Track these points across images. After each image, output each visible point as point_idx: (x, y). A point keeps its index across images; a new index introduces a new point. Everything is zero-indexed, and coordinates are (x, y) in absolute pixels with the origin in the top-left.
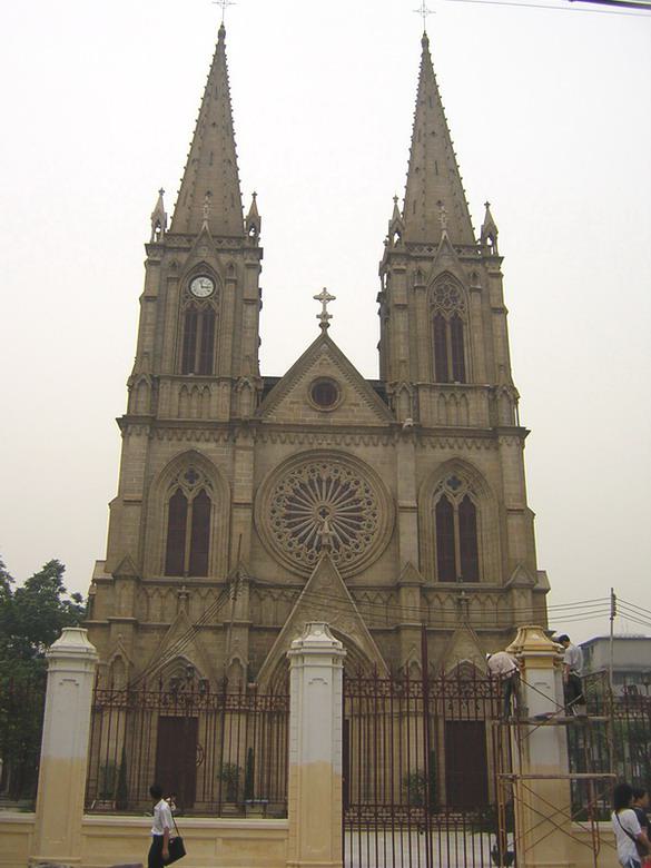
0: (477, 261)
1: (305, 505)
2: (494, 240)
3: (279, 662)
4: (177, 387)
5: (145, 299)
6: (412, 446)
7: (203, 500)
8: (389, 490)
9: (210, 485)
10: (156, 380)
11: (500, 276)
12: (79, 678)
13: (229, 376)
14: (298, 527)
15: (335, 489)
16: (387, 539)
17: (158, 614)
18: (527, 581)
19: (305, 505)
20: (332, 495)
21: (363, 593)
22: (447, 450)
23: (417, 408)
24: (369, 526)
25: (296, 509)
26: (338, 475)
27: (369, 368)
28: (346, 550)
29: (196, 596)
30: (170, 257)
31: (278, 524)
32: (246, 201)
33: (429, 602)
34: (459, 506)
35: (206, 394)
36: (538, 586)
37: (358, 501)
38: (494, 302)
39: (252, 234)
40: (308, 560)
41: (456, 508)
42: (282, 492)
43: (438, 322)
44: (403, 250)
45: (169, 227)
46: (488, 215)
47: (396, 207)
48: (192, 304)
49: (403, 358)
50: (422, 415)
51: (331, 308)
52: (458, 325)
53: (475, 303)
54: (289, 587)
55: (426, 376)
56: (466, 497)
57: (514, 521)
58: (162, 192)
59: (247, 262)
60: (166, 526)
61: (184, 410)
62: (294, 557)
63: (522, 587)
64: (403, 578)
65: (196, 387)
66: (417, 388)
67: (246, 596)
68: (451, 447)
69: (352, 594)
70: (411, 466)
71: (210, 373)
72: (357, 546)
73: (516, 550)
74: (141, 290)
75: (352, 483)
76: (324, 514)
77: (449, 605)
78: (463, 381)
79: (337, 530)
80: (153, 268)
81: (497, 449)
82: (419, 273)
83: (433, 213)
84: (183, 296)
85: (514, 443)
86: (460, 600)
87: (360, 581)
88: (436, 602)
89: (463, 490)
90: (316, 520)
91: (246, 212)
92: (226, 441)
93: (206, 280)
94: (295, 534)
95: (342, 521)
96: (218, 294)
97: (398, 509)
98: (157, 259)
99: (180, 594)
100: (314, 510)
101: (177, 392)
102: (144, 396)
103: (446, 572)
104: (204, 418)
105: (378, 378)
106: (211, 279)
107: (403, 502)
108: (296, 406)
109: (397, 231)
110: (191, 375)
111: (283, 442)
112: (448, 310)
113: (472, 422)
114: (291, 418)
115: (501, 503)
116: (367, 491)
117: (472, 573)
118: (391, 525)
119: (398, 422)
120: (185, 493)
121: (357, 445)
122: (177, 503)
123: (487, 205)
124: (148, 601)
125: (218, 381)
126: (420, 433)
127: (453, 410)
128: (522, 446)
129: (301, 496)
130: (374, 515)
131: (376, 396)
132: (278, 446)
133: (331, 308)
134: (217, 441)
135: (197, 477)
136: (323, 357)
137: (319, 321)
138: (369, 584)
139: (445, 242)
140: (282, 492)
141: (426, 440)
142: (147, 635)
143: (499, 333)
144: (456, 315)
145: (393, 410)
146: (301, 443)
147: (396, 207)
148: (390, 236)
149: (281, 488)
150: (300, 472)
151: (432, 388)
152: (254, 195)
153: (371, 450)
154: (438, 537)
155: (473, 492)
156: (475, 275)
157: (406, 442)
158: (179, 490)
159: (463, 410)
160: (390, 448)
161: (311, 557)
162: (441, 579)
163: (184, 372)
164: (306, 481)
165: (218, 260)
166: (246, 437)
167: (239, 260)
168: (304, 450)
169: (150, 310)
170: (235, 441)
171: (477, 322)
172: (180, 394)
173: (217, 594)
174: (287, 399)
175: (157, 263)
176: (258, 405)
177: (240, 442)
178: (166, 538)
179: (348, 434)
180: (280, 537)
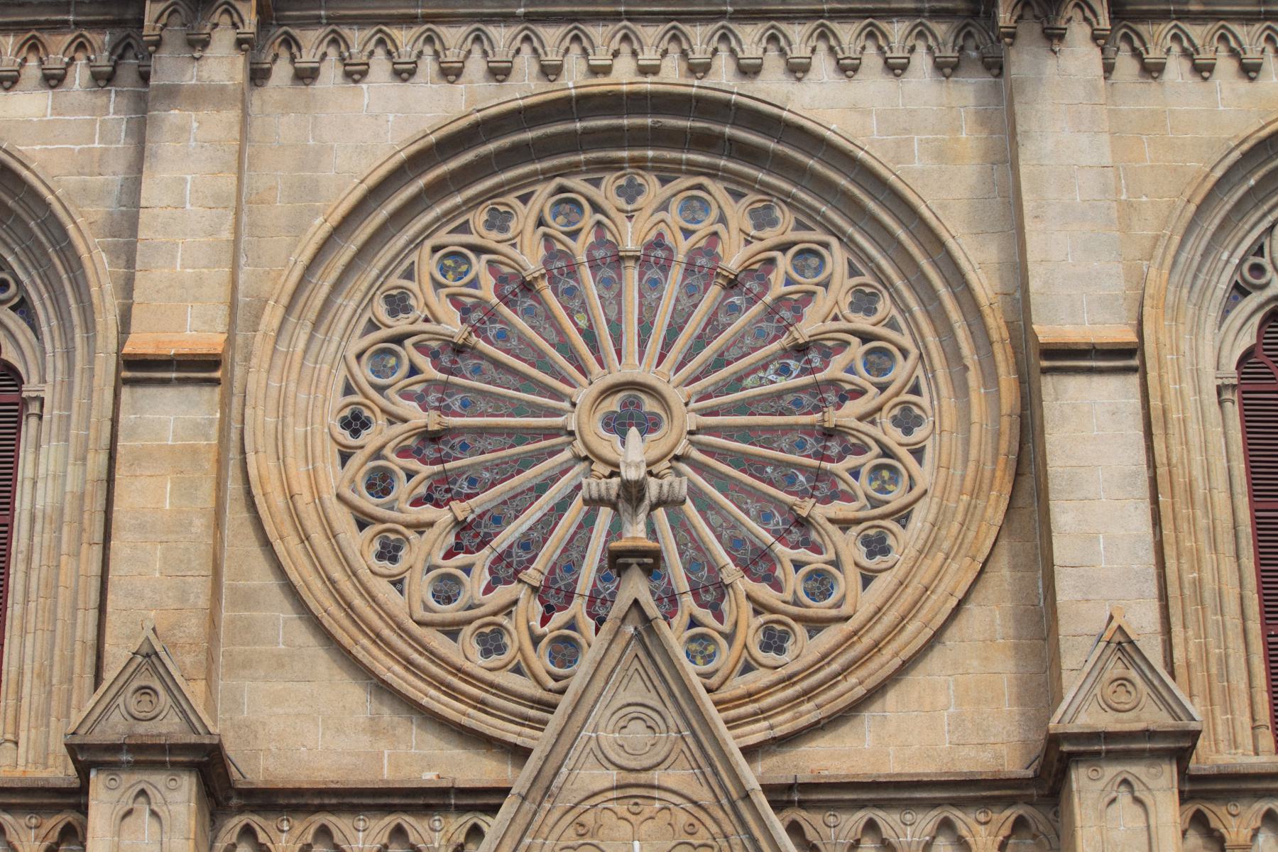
1: (526, 382)
8: (985, 286)
14: (485, 500)
15: (692, 291)
19: (526, 382)
21: (861, 817)
26: (703, 229)
28: (759, 608)
31: (380, 483)
40: (541, 662)
42: (401, 324)
62: (477, 663)
69: (795, 829)
72: (820, 584)
75: (784, 262)
90: (588, 459)
92: (102, 79)
107: (1047, 330)
111: (404, 74)
121: (798, 70)
130: (907, 421)
134: (53, 80)
138: (893, 766)
141: (1158, 37)
146: (499, 73)
150: (498, 221)
154: (1257, 522)
157: (1053, 37)
164: (531, 259)
166: (198, 44)
170: (145, 77)
180: (389, 552)
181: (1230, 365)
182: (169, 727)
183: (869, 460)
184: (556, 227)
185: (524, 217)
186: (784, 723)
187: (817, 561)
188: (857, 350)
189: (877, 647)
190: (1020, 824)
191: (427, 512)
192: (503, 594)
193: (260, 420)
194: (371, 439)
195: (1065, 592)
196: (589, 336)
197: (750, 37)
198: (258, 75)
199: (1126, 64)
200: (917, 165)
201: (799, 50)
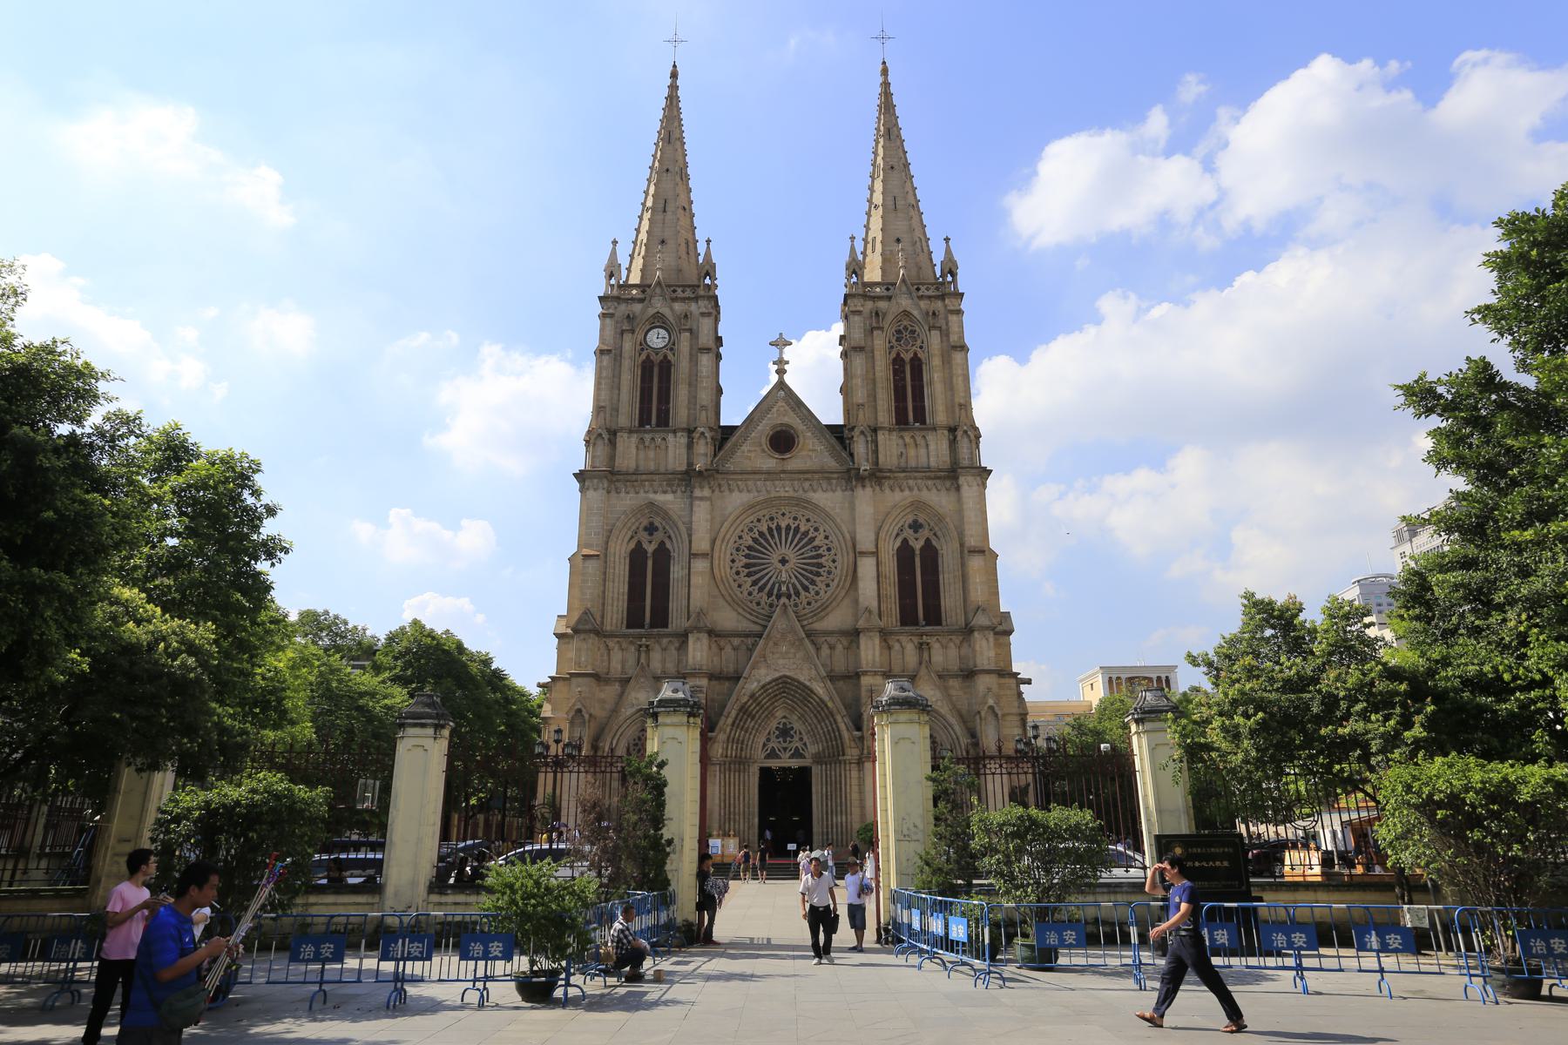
0: (937, 297)
1: (764, 554)
2: (953, 275)
3: (740, 710)
4: (634, 438)
5: (601, 353)
6: (871, 489)
7: (663, 555)
8: (848, 536)
9: (669, 537)
10: (613, 433)
11: (959, 312)
12: (428, 743)
13: (684, 426)
16: (848, 584)
17: (619, 667)
18: (987, 623)
19: (764, 554)
20: (792, 541)
22: (907, 493)
23: (876, 452)
24: (829, 573)
25: (755, 558)
26: (797, 523)
27: (830, 411)
29: (657, 647)
30: (623, 309)
31: (738, 573)
32: (701, 248)
33: (890, 648)
34: (921, 549)
35: (663, 447)
36: (1000, 628)
37: (817, 548)
38: (954, 338)
39: (708, 281)
40: (767, 608)
41: (918, 552)
43: (898, 362)
44: (860, 291)
45: (624, 278)
46: (948, 251)
47: (853, 249)
48: (648, 357)
49: (861, 401)
50: (880, 456)
51: (788, 353)
52: (917, 365)
53: (935, 339)
54: (747, 636)
55: (885, 416)
56: (928, 540)
57: (975, 563)
58: (615, 242)
59: (701, 310)
60: (627, 579)
61: (642, 463)
62: (755, 608)
63: (983, 628)
64: (861, 624)
65: (653, 439)
66: (875, 430)
67: (705, 647)
68: (911, 489)
69: (813, 643)
70: (870, 510)
71: (667, 425)
72: (817, 593)
73: (978, 594)
74: (595, 343)
75: (812, 530)
76: (783, 561)
77: (910, 648)
78: (923, 422)
79: (796, 577)
80: (608, 321)
81: (958, 489)
82: (877, 314)
83: (891, 251)
84: (638, 348)
85: (975, 483)
86: (921, 644)
87: (818, 626)
88: (897, 646)
89: (925, 533)
91: (701, 259)
93: (661, 330)
94: (754, 583)
95: (803, 569)
96: (674, 344)
97: (858, 554)
98: (611, 311)
99: (640, 646)
100: (775, 558)
101: (633, 446)
102: (602, 449)
103: (908, 617)
104: (662, 470)
105: (841, 422)
106: (667, 330)
108: (753, 455)
109: (854, 272)
110: (648, 427)
112: (907, 351)
113: (933, 464)
114: (748, 466)
115: (962, 545)
116: (826, 537)
117: (934, 616)
118: (850, 573)
119: (856, 466)
120: (645, 546)
122: (637, 557)
123: (947, 240)
124: (609, 655)
125: (675, 432)
126: (878, 476)
127: (912, 452)
128: (985, 488)
129: (760, 544)
130: (834, 561)
131: (834, 441)
132: (736, 494)
133: (788, 353)
134: (674, 492)
135: (656, 529)
136: (780, 404)
137: (776, 367)
139: (903, 281)
140: (741, 542)
141: (886, 483)
142: (607, 688)
143: (960, 372)
144: (915, 354)
145: (852, 455)
146: (758, 492)
147: (853, 249)
148: (849, 277)
149: (740, 537)
150: (759, 520)
151: (890, 430)
152: (708, 242)
153: (830, 494)
155: (935, 534)
156: (934, 314)
157: (864, 486)
158: (639, 543)
159: (923, 451)
160: (848, 493)
161: (771, 606)
162: (901, 625)
163: (642, 424)
164: (764, 529)
165: (672, 309)
166: (702, 488)
167: (693, 307)
168: (762, 498)
169: (605, 363)
171: (936, 362)
172: (637, 448)
173: (677, 645)
174: (745, 448)
175: (611, 316)
176: (715, 455)
177: (697, 493)
178: (626, 590)
179: (806, 479)
180: (740, 586)
181: (895, 549)
182: (702, 625)
183: (826, 569)
184: (770, 523)
185: (763, 521)
186: (810, 621)
187: (817, 589)
188: (825, 548)
189: (827, 607)
190: (852, 641)
191: (746, 578)
192: (760, 594)
193: (716, 562)
194: (736, 564)
195: (861, 599)
196: (775, 544)
197: (807, 485)
198: (713, 491)
199: (878, 488)
200: (837, 511)
201: (815, 487)
